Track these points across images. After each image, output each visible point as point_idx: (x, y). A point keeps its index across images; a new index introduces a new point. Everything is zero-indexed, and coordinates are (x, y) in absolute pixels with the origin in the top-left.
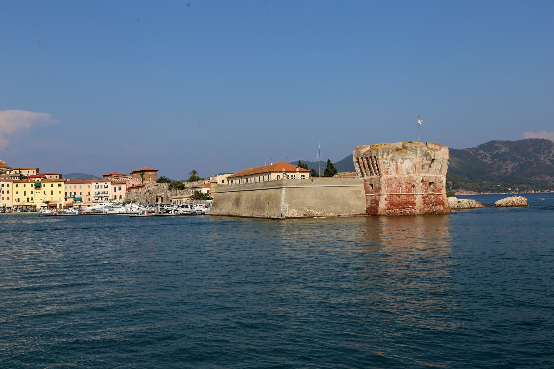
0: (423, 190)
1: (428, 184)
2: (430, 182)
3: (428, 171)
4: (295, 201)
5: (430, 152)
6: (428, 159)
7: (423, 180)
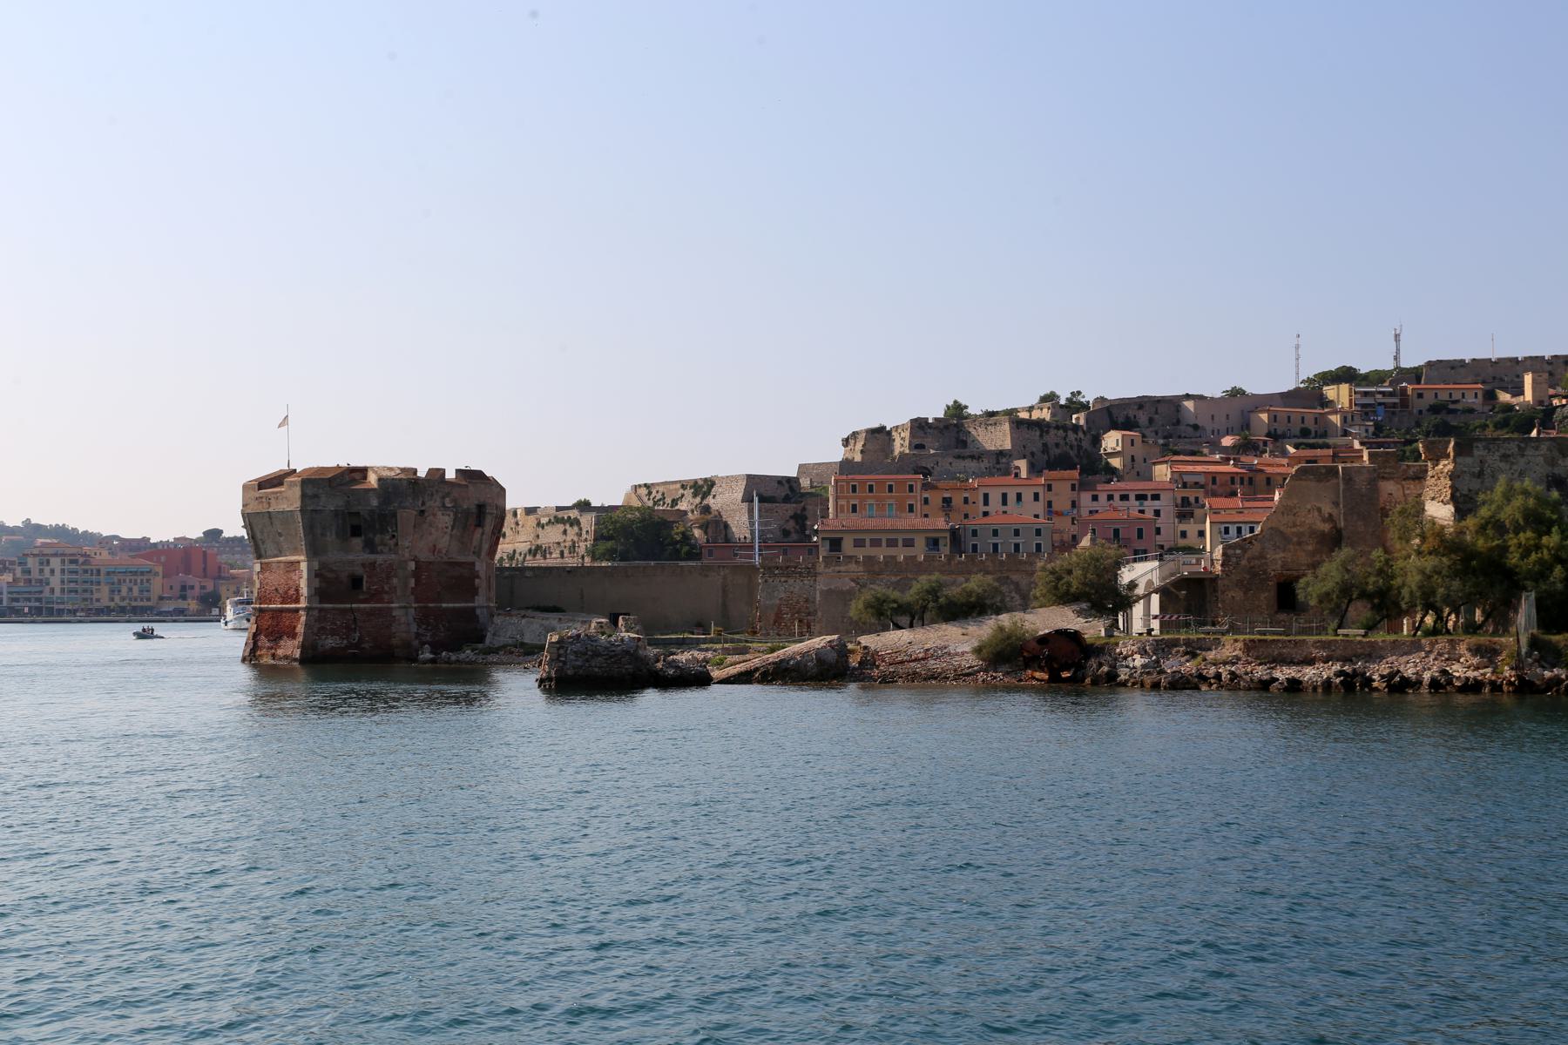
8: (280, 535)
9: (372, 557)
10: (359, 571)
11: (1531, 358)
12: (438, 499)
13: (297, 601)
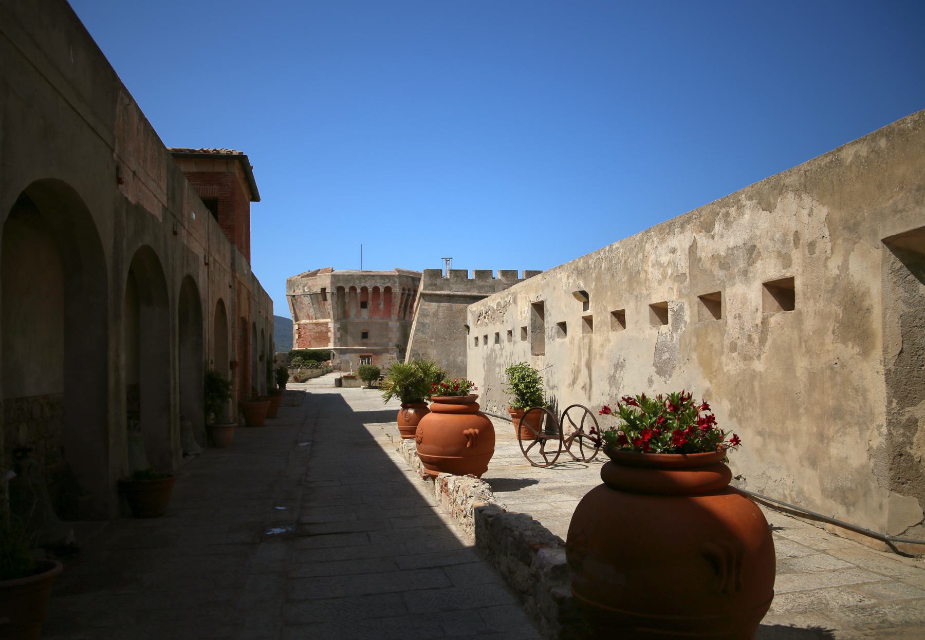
12: (301, 288)
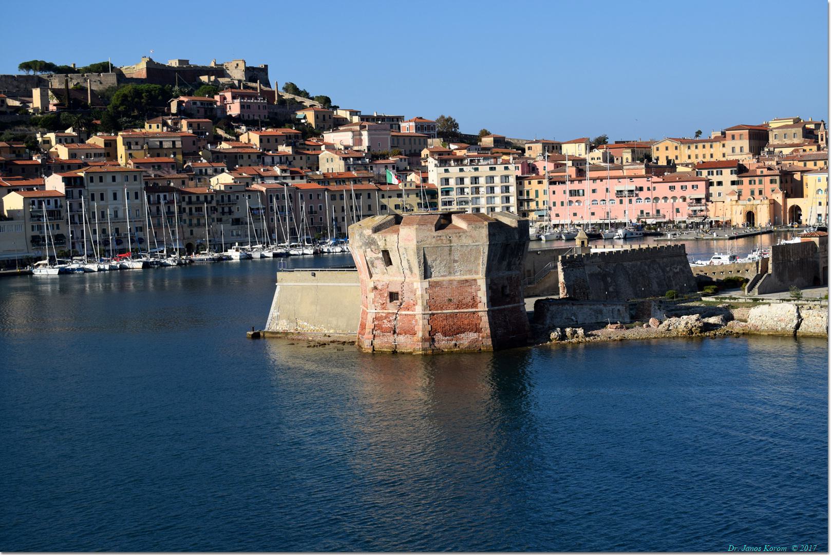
0: (376, 305)
1: (386, 295)
2: (391, 291)
3: (385, 271)
4: (288, 306)
5: (376, 237)
6: (373, 250)
7: (375, 288)
8: (455, 261)
9: (510, 273)
10: (506, 283)
11: (5, 76)
13: (474, 305)
